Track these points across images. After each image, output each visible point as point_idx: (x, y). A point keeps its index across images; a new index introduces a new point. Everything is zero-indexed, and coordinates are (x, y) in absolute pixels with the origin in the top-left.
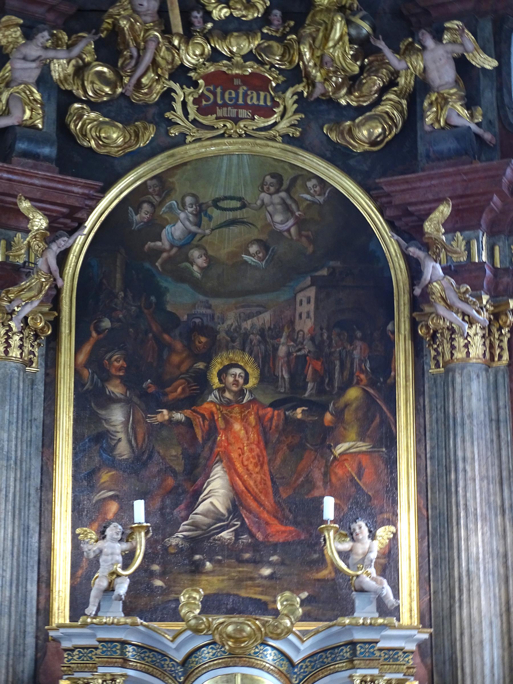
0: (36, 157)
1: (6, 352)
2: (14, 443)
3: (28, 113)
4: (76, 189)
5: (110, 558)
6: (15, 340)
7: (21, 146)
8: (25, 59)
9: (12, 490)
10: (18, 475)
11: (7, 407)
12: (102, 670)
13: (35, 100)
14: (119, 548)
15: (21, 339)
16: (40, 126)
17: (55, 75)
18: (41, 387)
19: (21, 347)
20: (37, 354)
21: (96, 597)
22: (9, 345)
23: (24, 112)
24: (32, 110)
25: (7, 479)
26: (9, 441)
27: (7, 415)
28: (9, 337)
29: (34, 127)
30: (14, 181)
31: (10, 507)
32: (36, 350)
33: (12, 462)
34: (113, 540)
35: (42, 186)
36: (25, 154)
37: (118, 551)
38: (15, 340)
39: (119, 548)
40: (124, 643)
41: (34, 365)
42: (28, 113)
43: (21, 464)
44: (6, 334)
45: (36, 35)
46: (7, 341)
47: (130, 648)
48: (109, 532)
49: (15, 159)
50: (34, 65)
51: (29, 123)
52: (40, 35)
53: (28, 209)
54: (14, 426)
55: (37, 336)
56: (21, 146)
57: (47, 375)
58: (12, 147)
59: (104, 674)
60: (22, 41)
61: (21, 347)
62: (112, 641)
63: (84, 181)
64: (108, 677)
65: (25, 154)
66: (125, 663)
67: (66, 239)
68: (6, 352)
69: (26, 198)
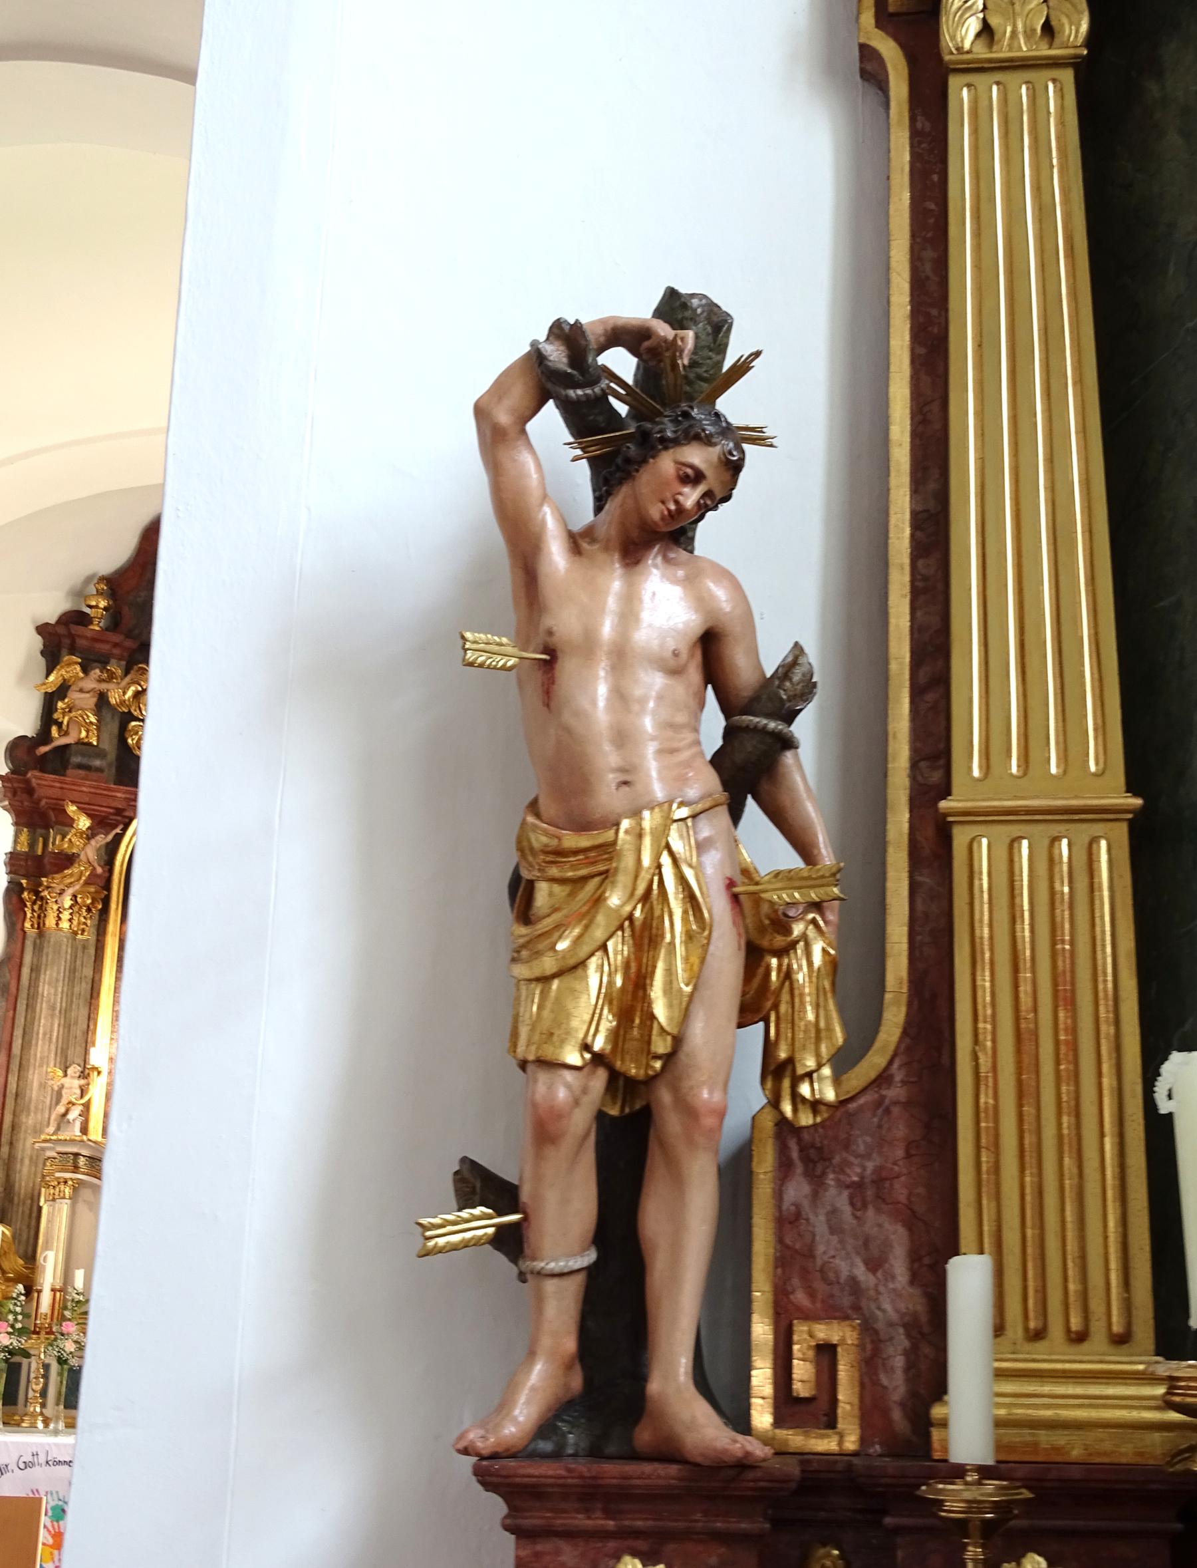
0: (88, 768)
1: (57, 924)
2: (60, 996)
3: (84, 734)
4: (119, 795)
5: (68, 1091)
6: (66, 916)
7: (76, 759)
8: (81, 691)
9: (55, 1034)
10: (62, 1022)
11: (55, 968)
12: (58, 1175)
13: (91, 722)
14: (77, 1083)
15: (71, 914)
16: (95, 743)
17: (113, 701)
18: (92, 951)
19: (70, 920)
20: (89, 925)
21: (55, 1120)
22: (60, 919)
23: (80, 732)
24: (88, 731)
25: (52, 1025)
26: (56, 995)
27: (55, 975)
28: (60, 912)
29: (90, 744)
30: (66, 789)
31: (53, 1047)
32: (89, 922)
33: (57, 1012)
34: (72, 1077)
35: (90, 793)
36: (80, 766)
37: (77, 1086)
38: (66, 916)
39: (77, 1083)
40: (76, 1155)
41: (86, 934)
42: (84, 734)
43: (65, 1013)
44: (58, 910)
45: (90, 671)
46: (58, 916)
47: (82, 1159)
48: (70, 1071)
49: (69, 772)
50: (88, 695)
51: (86, 740)
52: (93, 672)
53: (74, 812)
54: (61, 984)
55: (89, 910)
56: (76, 759)
57: (98, 940)
58: (68, 761)
59: (59, 1178)
60: (81, 675)
61: (70, 920)
62: (66, 1154)
63: (125, 788)
64: (62, 1180)
65: (80, 766)
66: (76, 1169)
67: (103, 836)
68: (57, 924)
69: (73, 802)
